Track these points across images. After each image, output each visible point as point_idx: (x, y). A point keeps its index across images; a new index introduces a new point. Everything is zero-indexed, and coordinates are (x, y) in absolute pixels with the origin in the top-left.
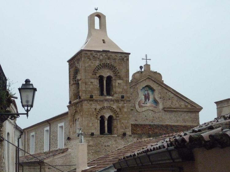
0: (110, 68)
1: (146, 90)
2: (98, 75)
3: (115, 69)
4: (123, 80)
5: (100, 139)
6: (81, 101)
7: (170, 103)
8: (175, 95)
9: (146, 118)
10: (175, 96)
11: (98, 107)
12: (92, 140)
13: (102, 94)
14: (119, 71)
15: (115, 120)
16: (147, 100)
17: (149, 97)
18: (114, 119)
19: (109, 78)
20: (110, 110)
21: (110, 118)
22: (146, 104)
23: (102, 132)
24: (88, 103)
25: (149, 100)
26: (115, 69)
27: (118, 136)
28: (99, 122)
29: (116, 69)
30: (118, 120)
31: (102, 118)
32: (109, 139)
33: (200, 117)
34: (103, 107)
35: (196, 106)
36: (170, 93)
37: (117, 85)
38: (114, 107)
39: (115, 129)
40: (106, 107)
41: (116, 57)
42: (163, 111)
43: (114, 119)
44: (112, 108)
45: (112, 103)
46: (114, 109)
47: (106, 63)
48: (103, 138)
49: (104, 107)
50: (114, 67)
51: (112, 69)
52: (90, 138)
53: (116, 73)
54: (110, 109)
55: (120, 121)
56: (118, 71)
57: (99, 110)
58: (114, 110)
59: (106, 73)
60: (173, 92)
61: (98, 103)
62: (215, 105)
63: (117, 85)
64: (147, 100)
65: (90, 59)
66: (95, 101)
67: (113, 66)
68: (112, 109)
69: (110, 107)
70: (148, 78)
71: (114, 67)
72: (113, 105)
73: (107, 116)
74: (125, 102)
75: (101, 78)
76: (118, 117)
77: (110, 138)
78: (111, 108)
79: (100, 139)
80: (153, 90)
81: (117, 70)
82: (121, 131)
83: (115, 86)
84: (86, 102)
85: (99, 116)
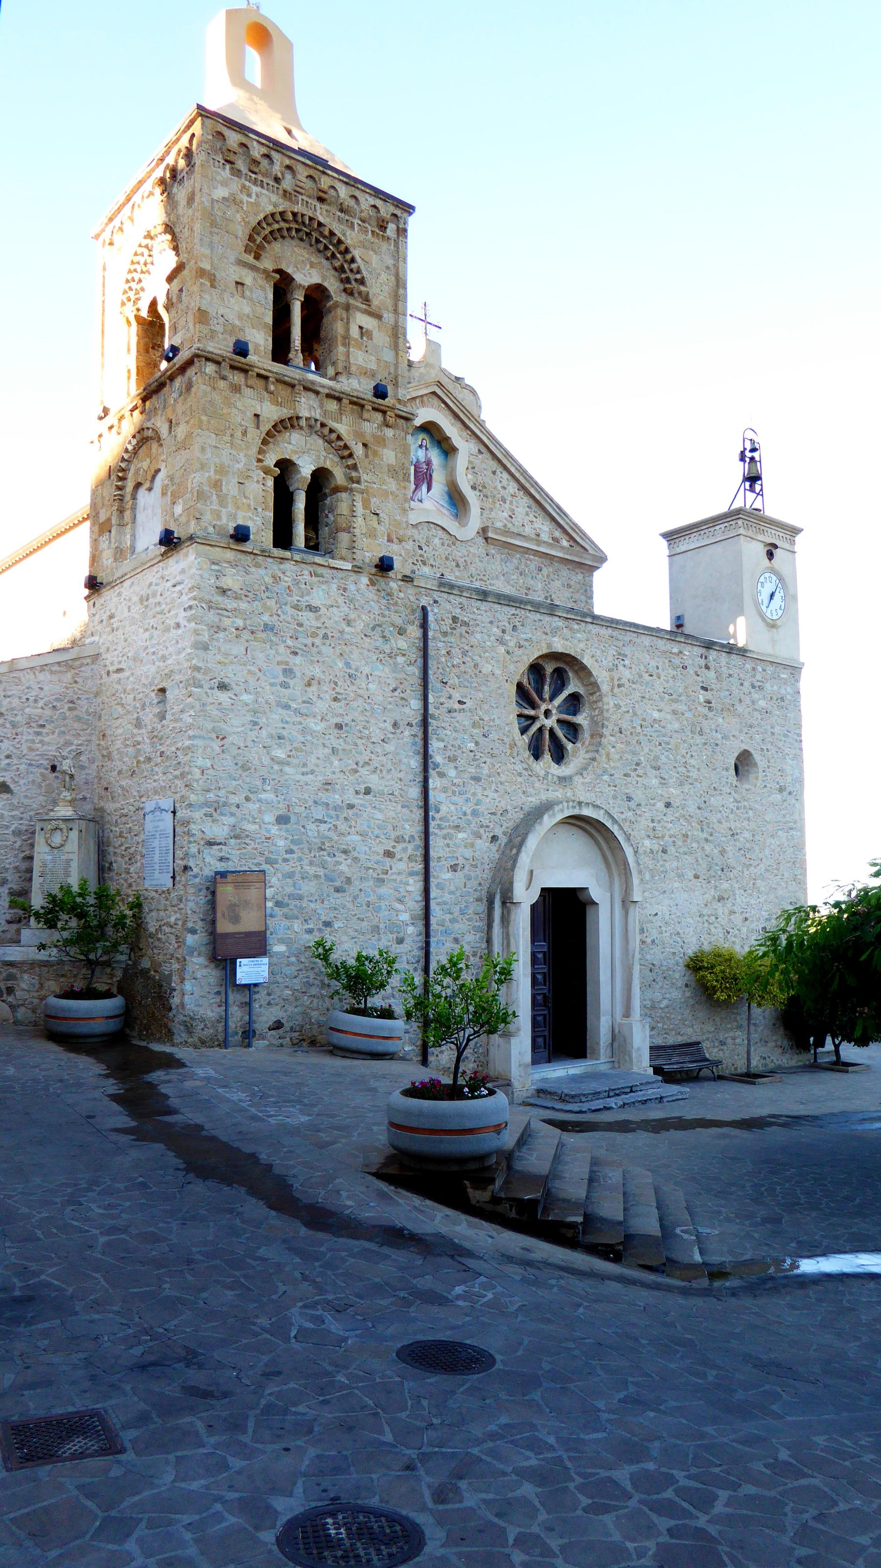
0: (326, 248)
1: (421, 446)
2: (268, 264)
3: (348, 257)
4: (379, 317)
5: (274, 567)
6: (183, 369)
7: (505, 514)
8: (522, 487)
9: (421, 556)
10: (522, 493)
11: (271, 412)
12: (233, 565)
13: (280, 352)
14: (365, 273)
15: (344, 495)
16: (424, 488)
17: (431, 476)
18: (337, 490)
19: (316, 301)
20: (321, 441)
21: (320, 476)
22: (421, 501)
23: (282, 537)
24: (224, 378)
25: (429, 488)
26: (348, 257)
27: (357, 570)
28: (270, 483)
29: (353, 260)
30: (358, 497)
31: (285, 466)
32: (316, 575)
33: (595, 588)
34: (290, 419)
35: (587, 547)
36: (505, 475)
37: (354, 332)
38: (343, 428)
39: (344, 537)
40: (303, 423)
41: (352, 202)
42: (481, 540)
43: (337, 490)
44: (331, 431)
45: (333, 406)
46: (339, 438)
47: (311, 219)
48: (288, 566)
49: (298, 418)
50: (342, 248)
51: (333, 256)
52: (229, 555)
53: (348, 280)
54: (323, 437)
55: (366, 504)
56: (359, 271)
57: (274, 427)
58: (341, 443)
59: (308, 272)
60: (517, 475)
61: (272, 393)
62: (664, 543)
63: (354, 332)
64: (424, 488)
65: (237, 173)
66: (259, 376)
67: (340, 242)
68: (333, 436)
69: (323, 425)
70: (434, 393)
71: (342, 248)
72: (340, 421)
73: (306, 469)
74: (391, 421)
75: (282, 285)
76: (358, 482)
77: (320, 570)
78: (326, 431)
79: (275, 567)
80: (447, 449)
81: (354, 266)
82: (370, 552)
83: (346, 337)
84: (210, 368)
85: (271, 460)
